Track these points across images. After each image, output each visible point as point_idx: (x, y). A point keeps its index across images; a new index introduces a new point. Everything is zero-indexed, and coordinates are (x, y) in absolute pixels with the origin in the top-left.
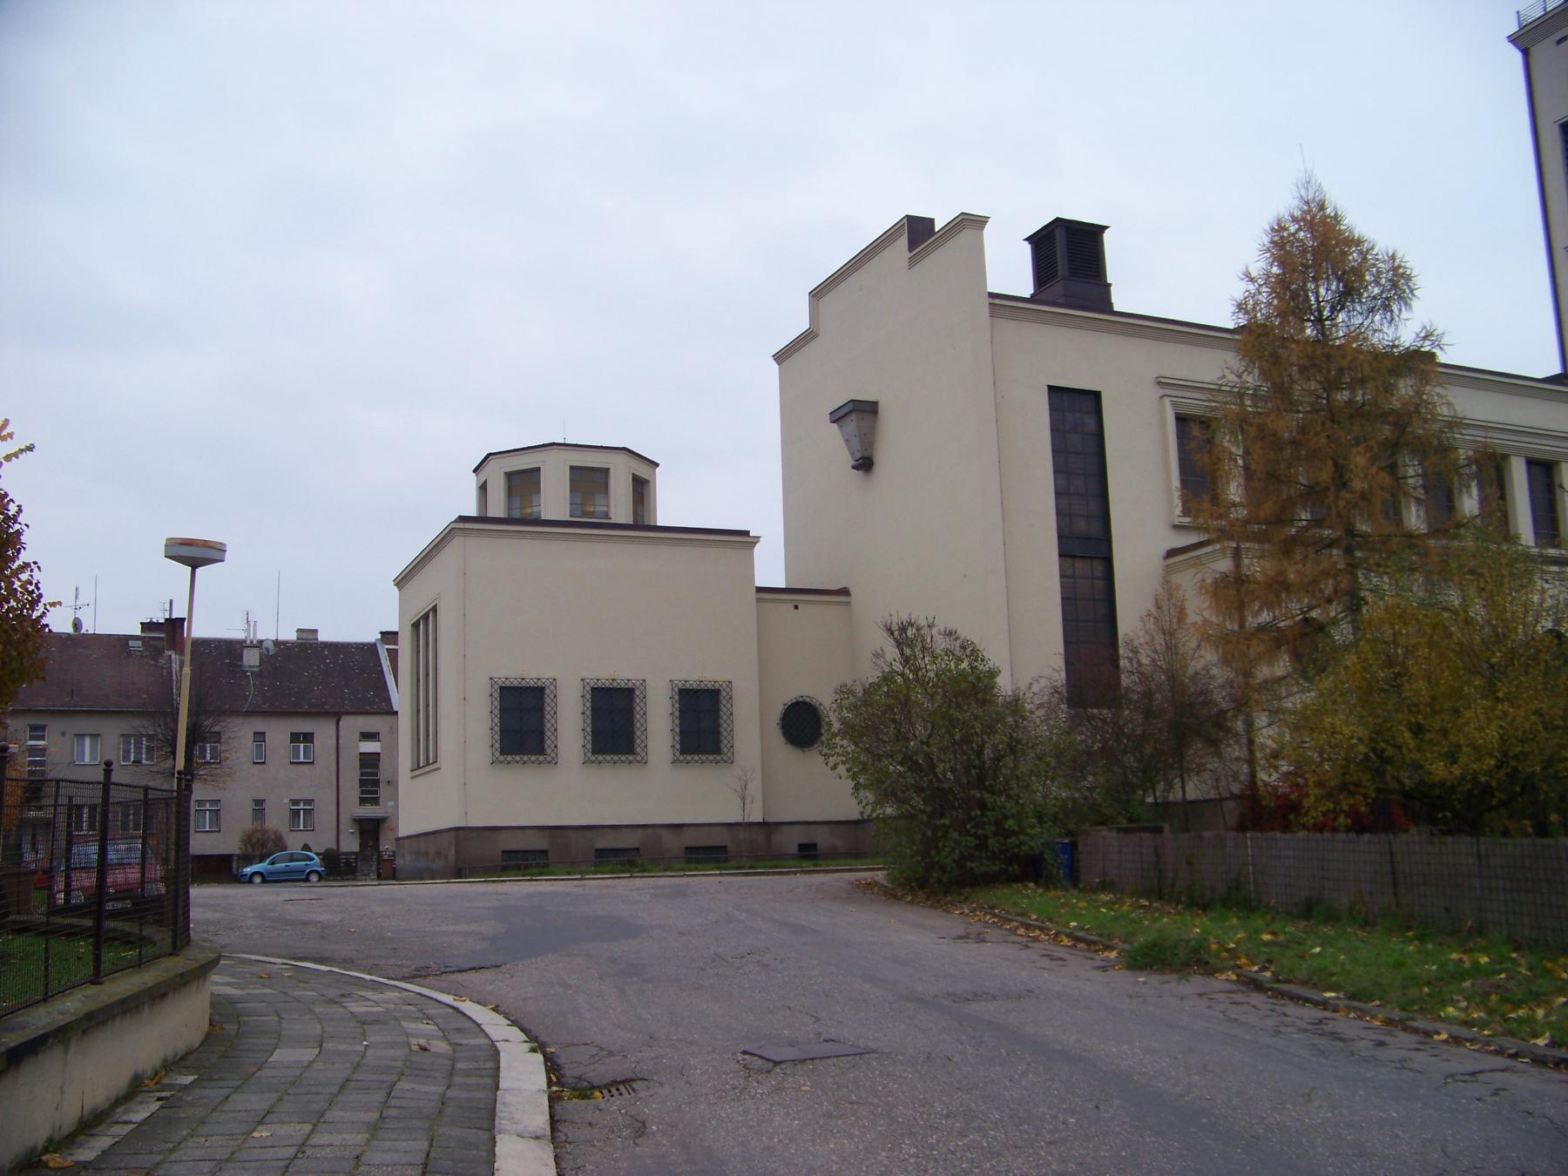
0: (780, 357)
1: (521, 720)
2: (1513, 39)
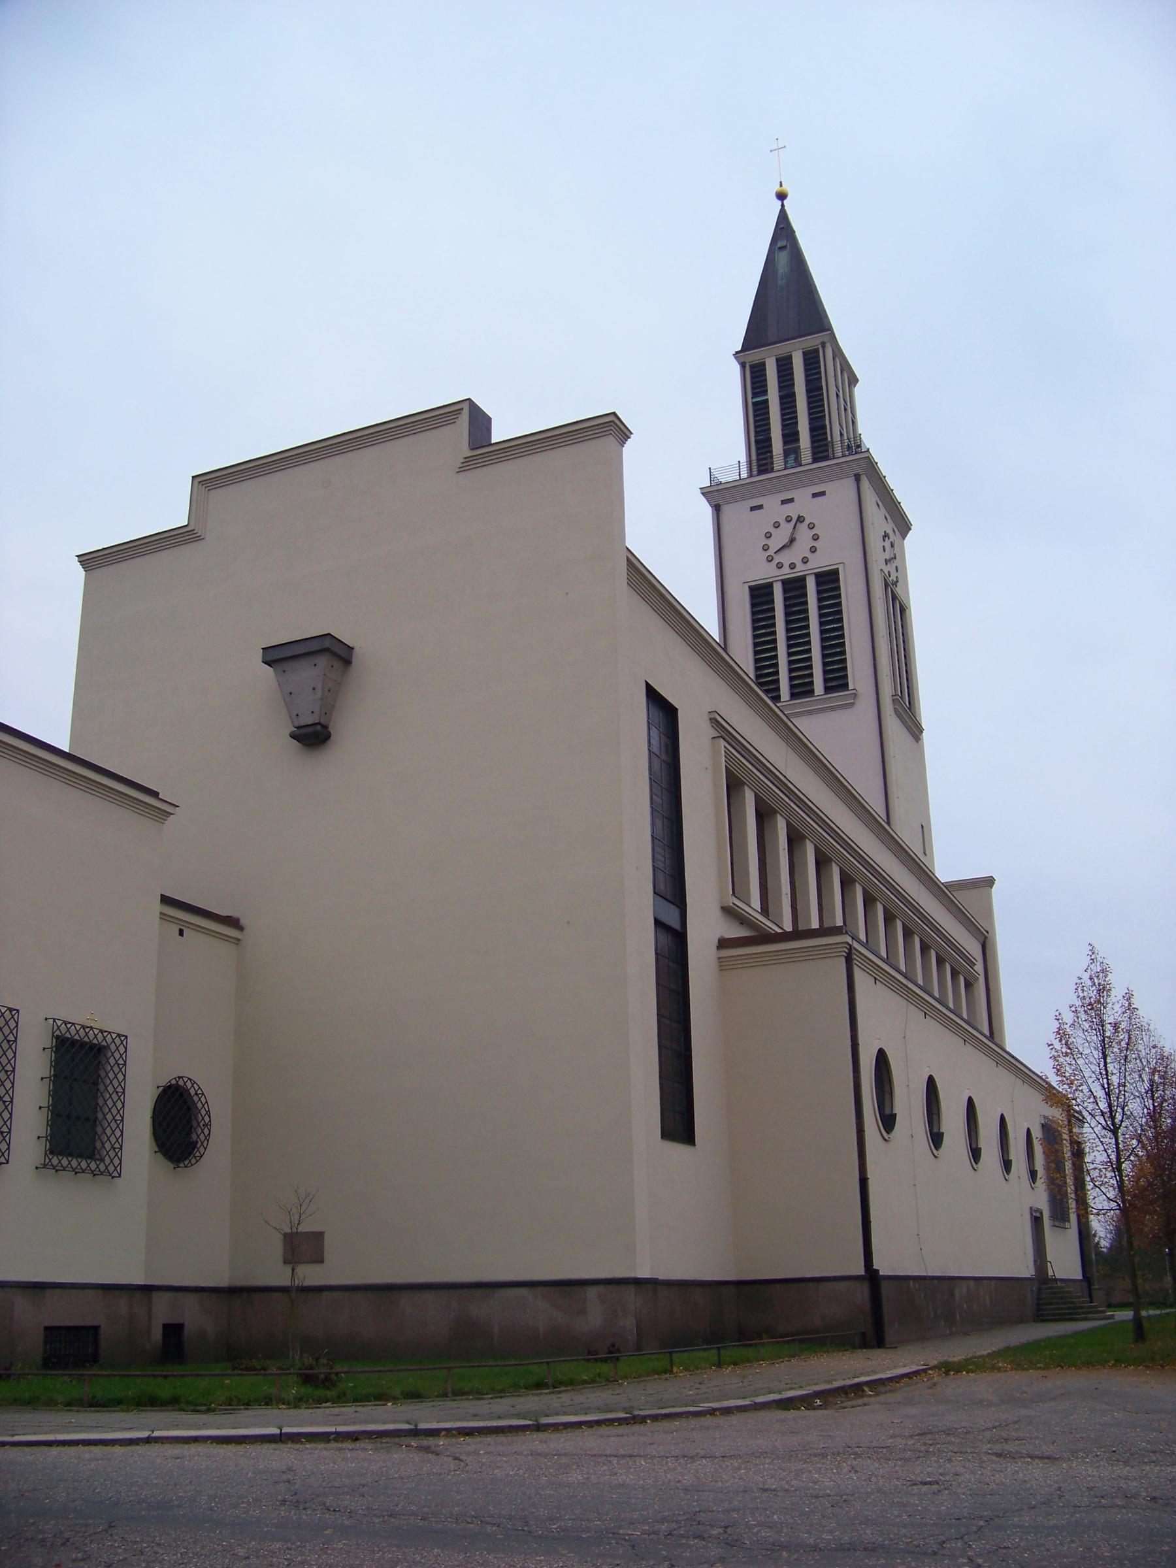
0: (89, 561)
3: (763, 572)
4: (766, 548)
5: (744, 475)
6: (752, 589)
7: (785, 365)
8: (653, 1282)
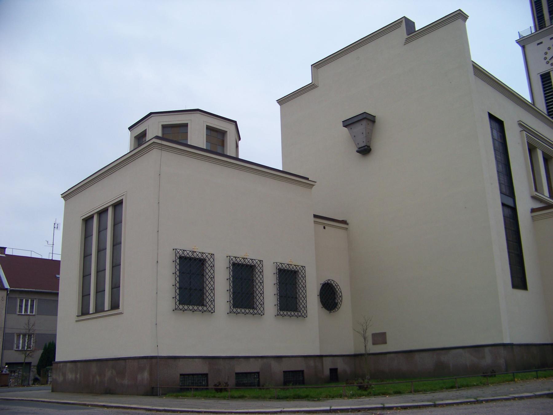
0: (281, 102)
1: (191, 280)
2: (518, 42)
4: (545, 59)
5: (533, 31)
6: (541, 76)
8: (511, 345)
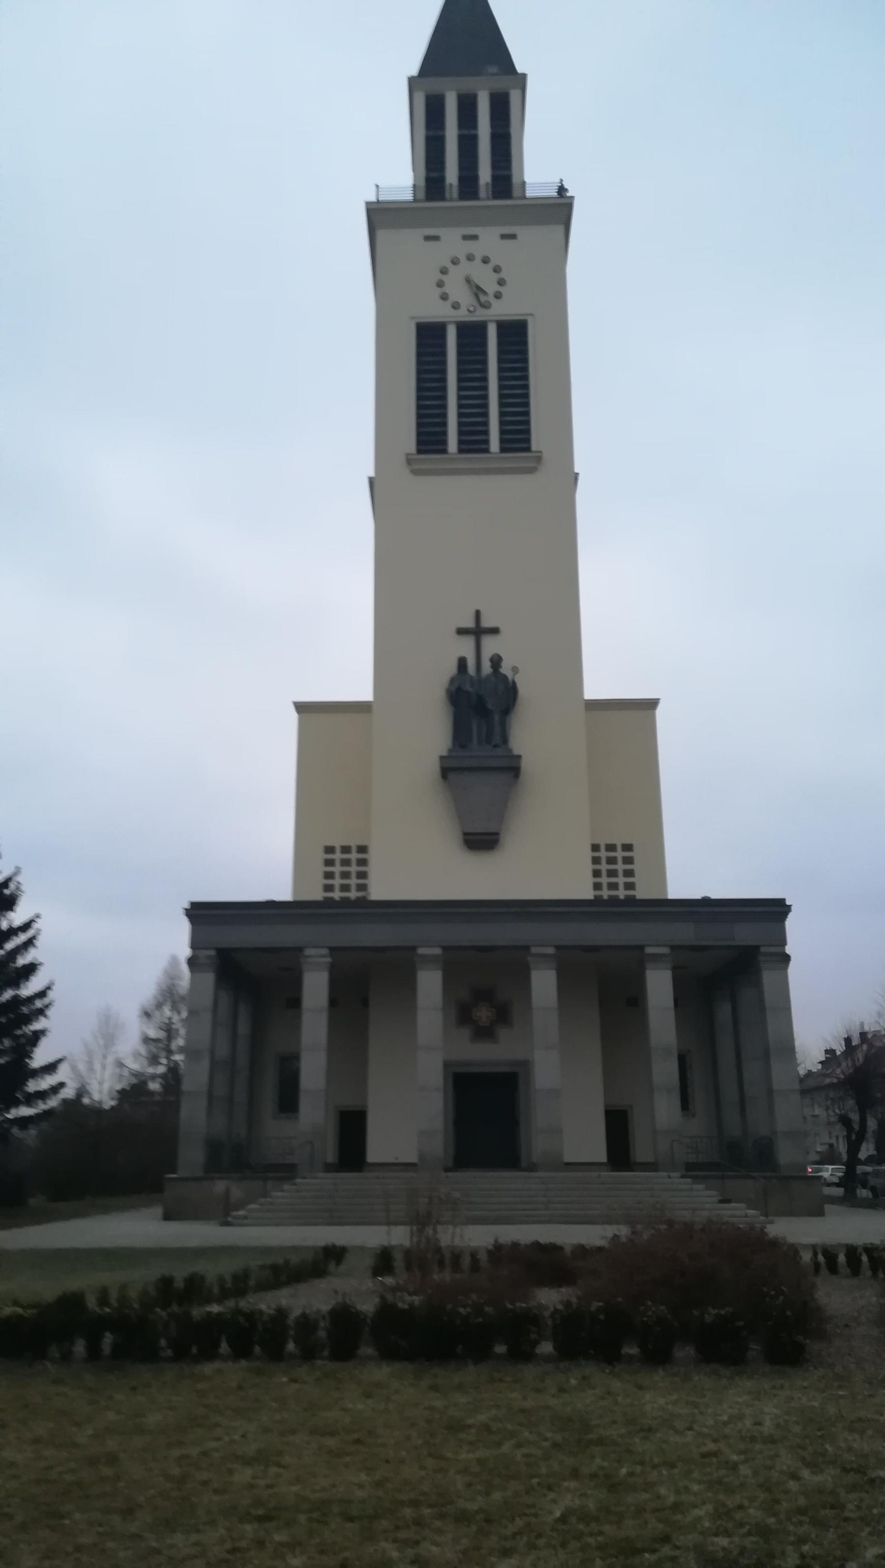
3: (436, 311)
7: (468, 106)
